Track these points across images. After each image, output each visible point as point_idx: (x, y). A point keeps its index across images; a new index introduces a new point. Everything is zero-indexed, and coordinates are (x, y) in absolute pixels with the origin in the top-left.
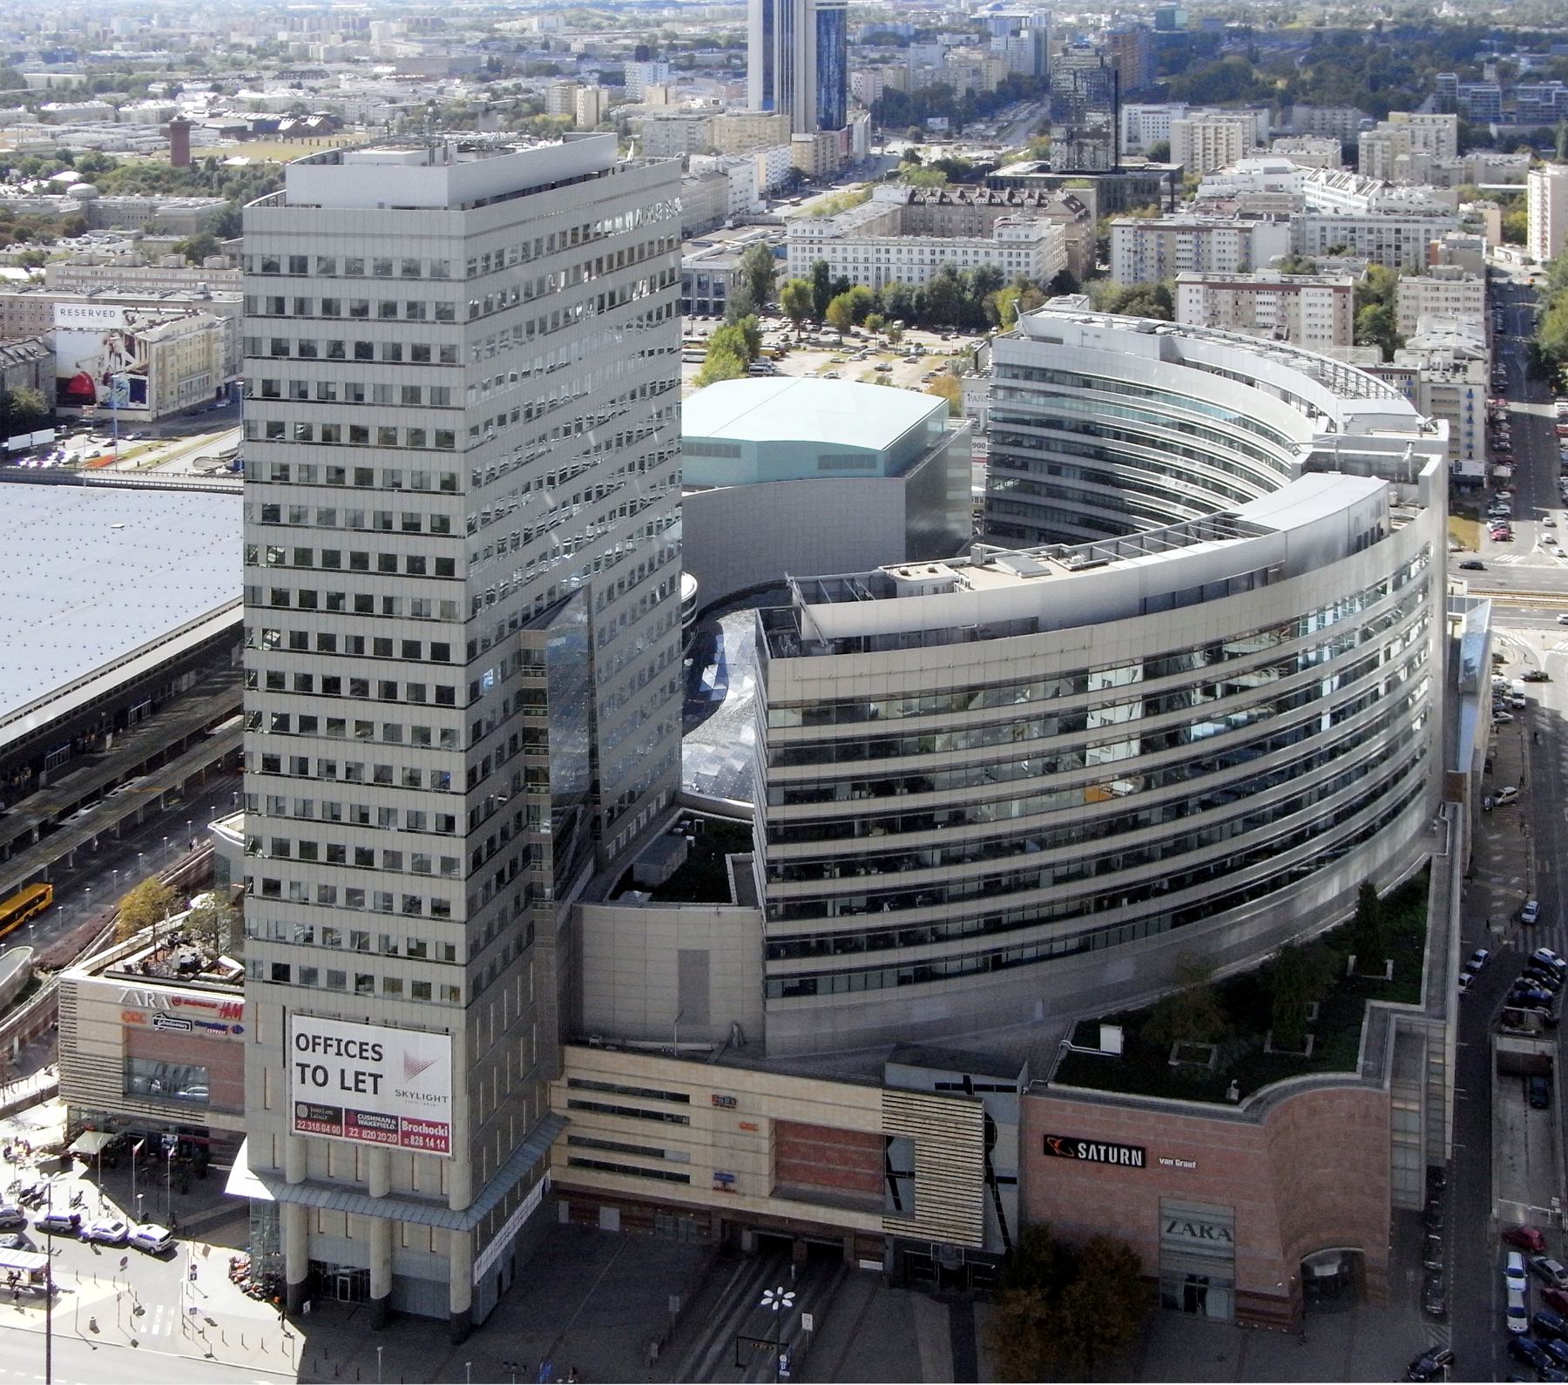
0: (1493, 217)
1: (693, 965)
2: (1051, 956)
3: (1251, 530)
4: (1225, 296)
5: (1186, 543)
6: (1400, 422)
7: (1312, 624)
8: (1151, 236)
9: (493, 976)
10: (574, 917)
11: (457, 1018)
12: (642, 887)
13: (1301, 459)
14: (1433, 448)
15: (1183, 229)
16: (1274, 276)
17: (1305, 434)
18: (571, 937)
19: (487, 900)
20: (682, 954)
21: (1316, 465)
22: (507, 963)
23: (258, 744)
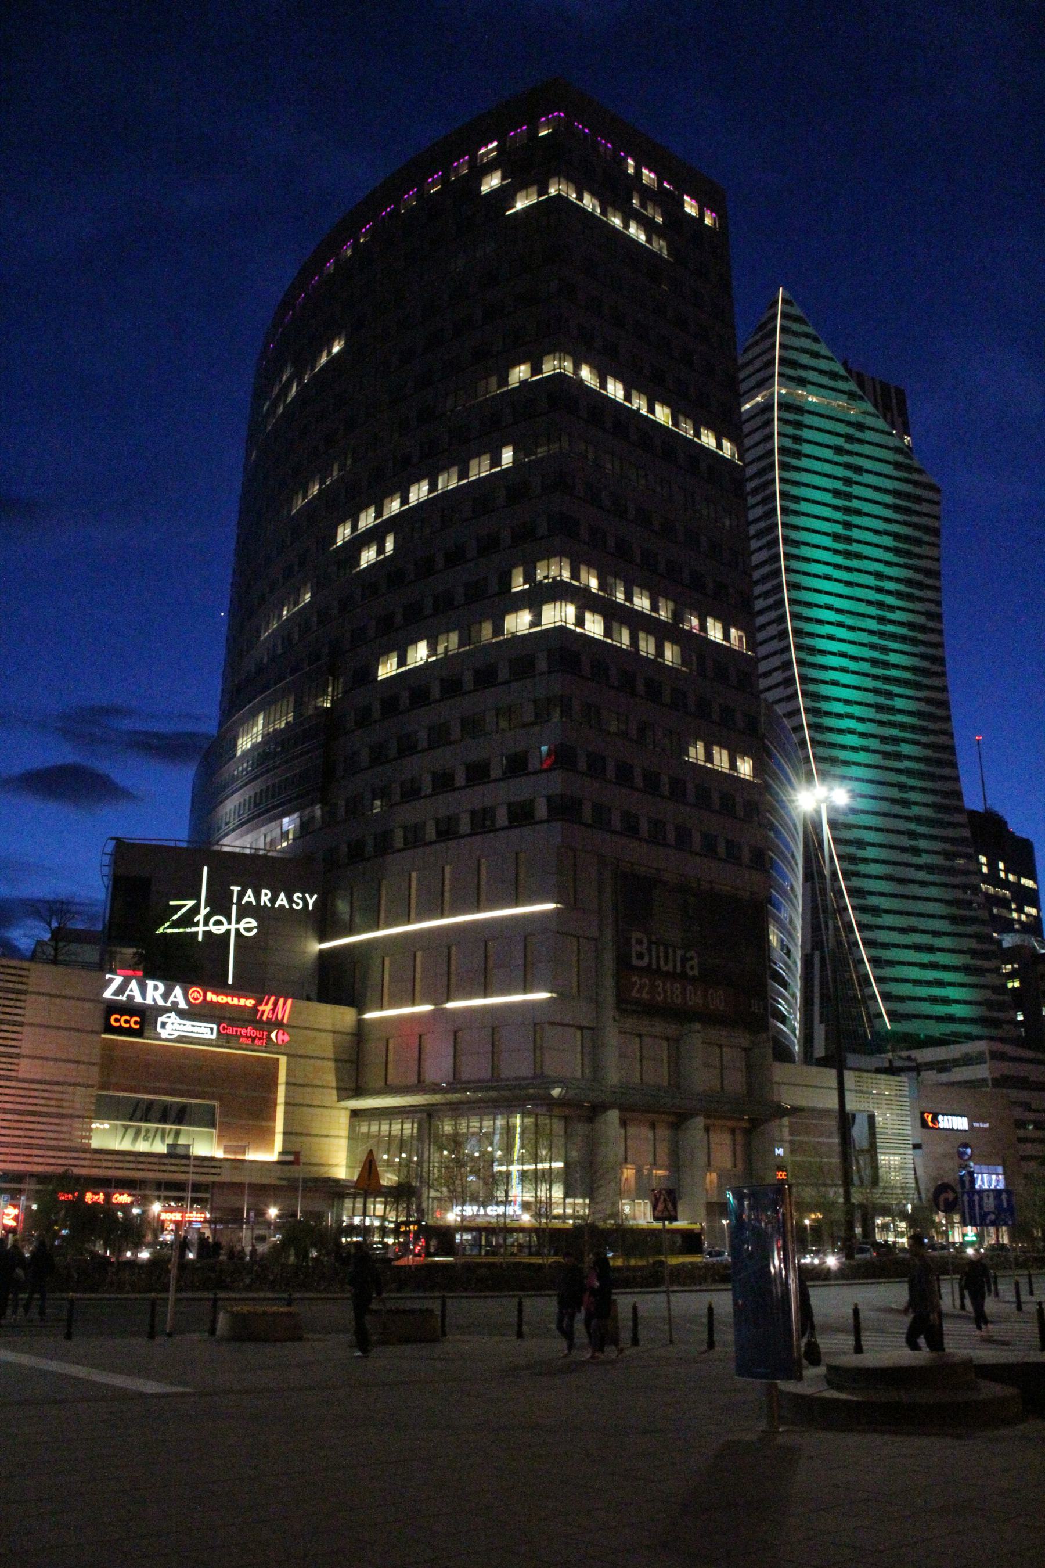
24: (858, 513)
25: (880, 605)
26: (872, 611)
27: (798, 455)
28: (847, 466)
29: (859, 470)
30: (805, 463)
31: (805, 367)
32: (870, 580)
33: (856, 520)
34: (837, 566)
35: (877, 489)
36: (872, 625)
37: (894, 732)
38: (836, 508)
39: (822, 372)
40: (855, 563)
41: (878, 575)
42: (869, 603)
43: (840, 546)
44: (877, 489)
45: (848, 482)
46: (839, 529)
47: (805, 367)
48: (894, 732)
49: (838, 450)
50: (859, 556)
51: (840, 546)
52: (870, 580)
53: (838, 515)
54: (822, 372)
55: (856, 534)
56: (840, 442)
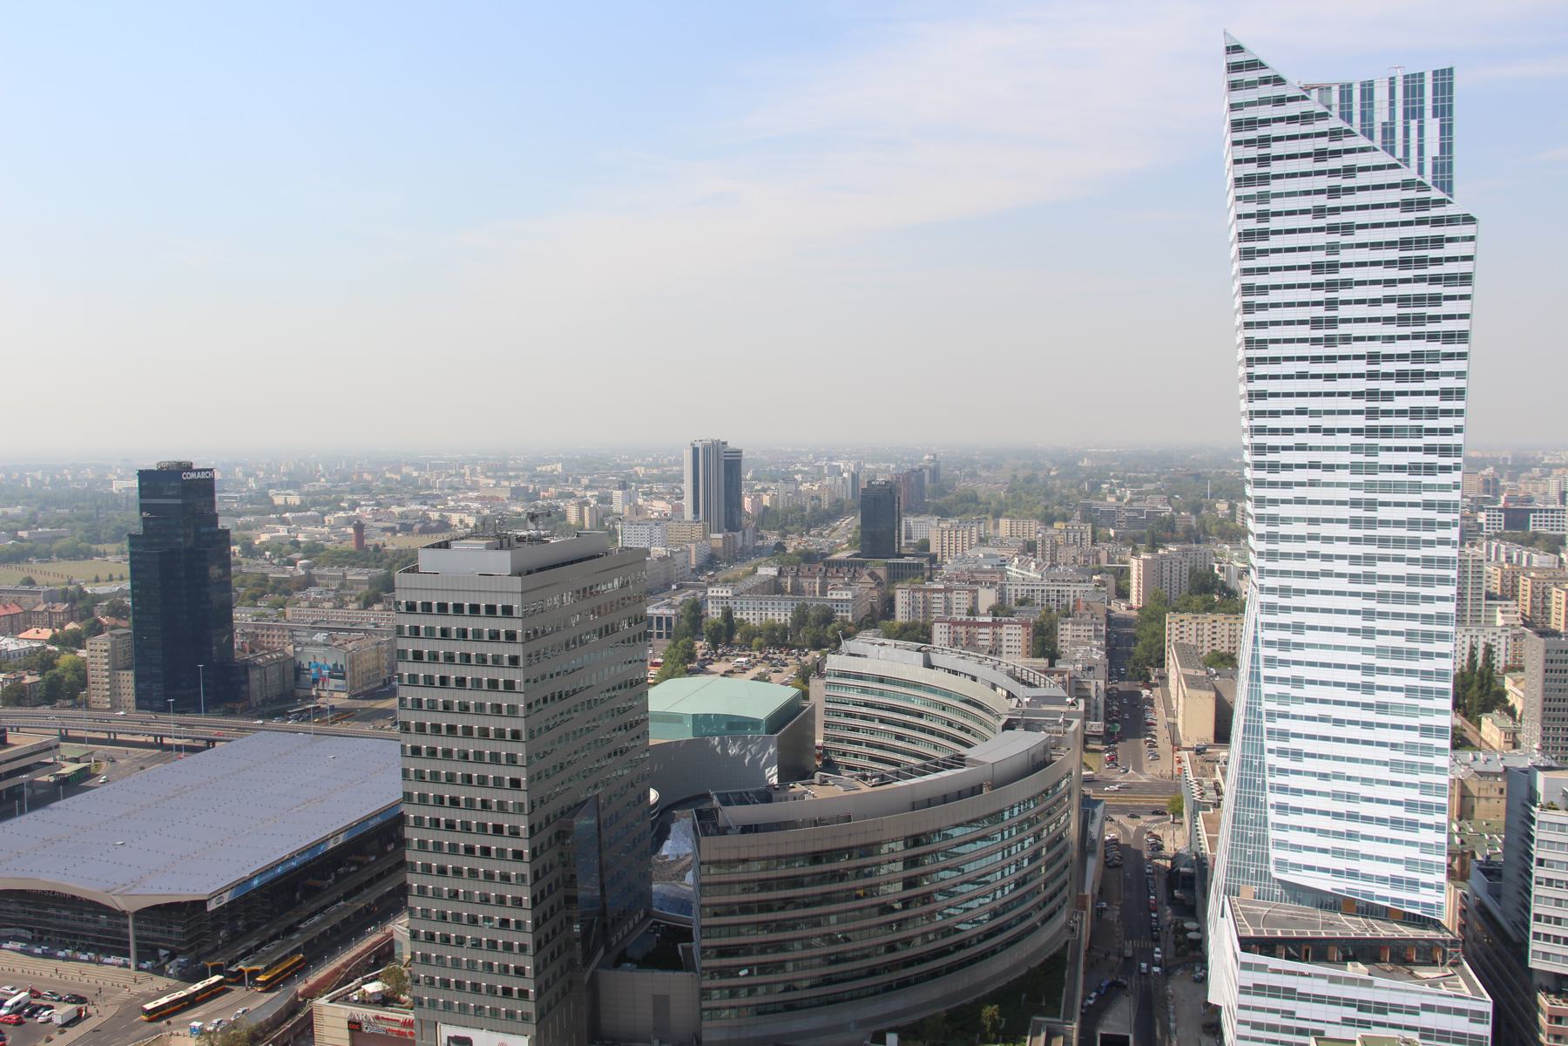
0: (1111, 581)
1: (661, 1003)
2: (858, 998)
3: (974, 762)
4: (962, 630)
5: (937, 771)
6: (1059, 701)
7: (1007, 815)
8: (919, 595)
9: (550, 1008)
10: (594, 975)
11: (532, 1029)
12: (630, 960)
13: (1003, 721)
14: (1076, 715)
15: (939, 591)
16: (989, 619)
17: (1006, 708)
18: (593, 986)
19: (545, 966)
20: (655, 997)
21: (1009, 726)
22: (557, 1001)
23: (414, 881)
24: (1347, 284)
25: (1372, 394)
26: (1361, 404)
27: (1264, 234)
28: (1332, 229)
29: (1347, 228)
30: (1274, 242)
31: (1265, 122)
32: (1362, 366)
33: (1343, 294)
34: (1316, 359)
35: (1376, 246)
36: (1360, 422)
37: (1373, 549)
38: (1317, 286)
39: (1291, 119)
40: (1342, 350)
41: (1373, 358)
42: (1358, 395)
43: (1320, 333)
44: (1376, 246)
45: (1333, 248)
46: (1320, 312)
47: (1265, 122)
48: (1373, 549)
49: (1319, 212)
50: (1346, 339)
51: (1320, 333)
52: (1362, 366)
53: (1321, 295)
54: (1291, 119)
55: (1343, 312)
56: (1321, 200)
